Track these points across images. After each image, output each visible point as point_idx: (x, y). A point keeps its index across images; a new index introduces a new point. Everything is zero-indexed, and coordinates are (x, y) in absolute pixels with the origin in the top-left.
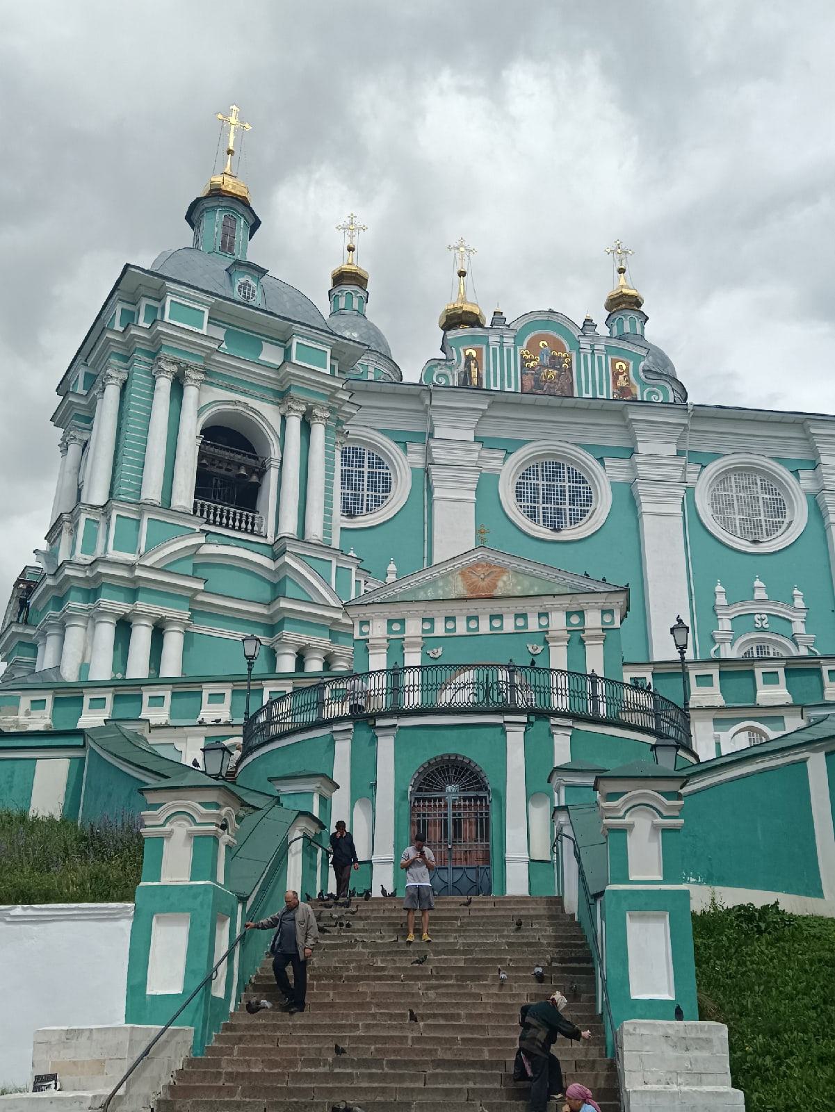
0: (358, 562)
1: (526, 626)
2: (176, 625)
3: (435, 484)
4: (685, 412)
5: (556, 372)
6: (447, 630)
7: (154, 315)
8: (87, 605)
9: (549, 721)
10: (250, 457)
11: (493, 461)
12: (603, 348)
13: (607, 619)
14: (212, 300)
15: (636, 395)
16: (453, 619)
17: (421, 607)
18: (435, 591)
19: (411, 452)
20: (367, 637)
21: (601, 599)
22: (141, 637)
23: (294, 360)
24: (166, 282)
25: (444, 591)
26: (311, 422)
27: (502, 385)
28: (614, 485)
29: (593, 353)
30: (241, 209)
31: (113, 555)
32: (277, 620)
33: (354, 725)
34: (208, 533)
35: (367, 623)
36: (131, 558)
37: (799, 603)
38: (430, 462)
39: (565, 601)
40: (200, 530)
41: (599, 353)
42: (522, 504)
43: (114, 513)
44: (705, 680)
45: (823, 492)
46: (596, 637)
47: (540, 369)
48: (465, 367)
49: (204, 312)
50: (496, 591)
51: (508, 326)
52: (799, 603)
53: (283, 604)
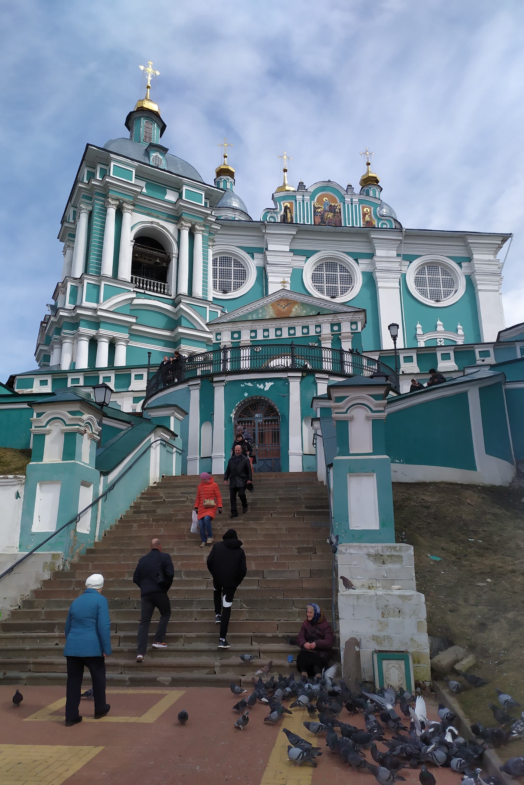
0: (222, 308)
1: (308, 333)
2: (122, 341)
3: (269, 274)
4: (401, 233)
5: (333, 214)
6: (264, 337)
7: (105, 173)
8: (73, 331)
9: (315, 375)
10: (162, 252)
12: (357, 200)
13: (354, 327)
14: (136, 164)
15: (375, 225)
16: (267, 330)
17: (249, 324)
18: (258, 315)
19: (256, 258)
20: (220, 341)
21: (350, 317)
22: (103, 348)
23: (184, 198)
24: (110, 154)
25: (262, 315)
26: (195, 233)
27: (304, 221)
28: (363, 273)
29: (352, 204)
30: (154, 118)
31: (85, 304)
32: (178, 339)
33: (201, 381)
34: (137, 292)
35: (220, 334)
36: (94, 305)
37: (460, 332)
38: (266, 262)
39: (330, 318)
40: (133, 291)
41: (355, 203)
42: (315, 284)
43: (86, 282)
44: (408, 359)
45: (474, 273)
46: (348, 338)
47: (324, 213)
48: (284, 212)
49: (132, 171)
50: (291, 314)
51: (307, 190)
52: (460, 332)
53: (180, 330)
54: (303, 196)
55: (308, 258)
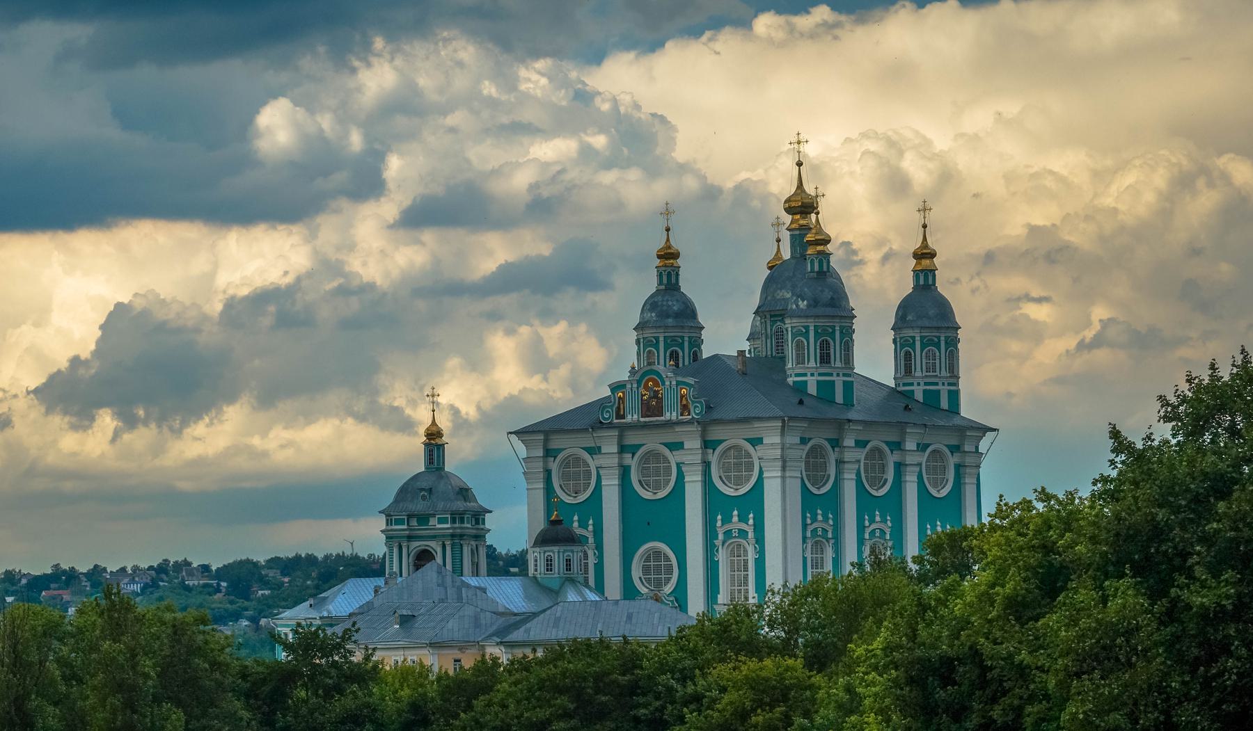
11: (627, 459)
54: (632, 384)
55: (633, 455)
